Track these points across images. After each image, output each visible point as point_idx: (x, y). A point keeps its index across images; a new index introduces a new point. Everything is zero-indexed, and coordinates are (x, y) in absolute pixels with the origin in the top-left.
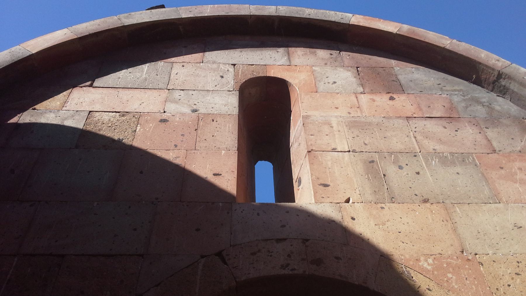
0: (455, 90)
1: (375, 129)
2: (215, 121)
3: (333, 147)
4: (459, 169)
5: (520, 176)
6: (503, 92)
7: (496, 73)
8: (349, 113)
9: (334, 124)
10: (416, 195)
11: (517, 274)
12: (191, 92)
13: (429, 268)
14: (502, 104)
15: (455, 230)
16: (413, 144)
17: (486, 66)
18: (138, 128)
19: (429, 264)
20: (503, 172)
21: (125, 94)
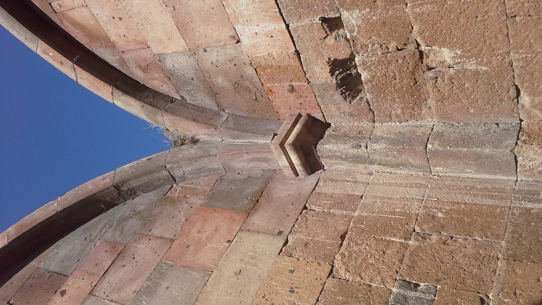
0: (101, 230)
4: (165, 284)
6: (133, 193)
7: (113, 188)
14: (141, 202)
17: (100, 191)
20: (192, 248)
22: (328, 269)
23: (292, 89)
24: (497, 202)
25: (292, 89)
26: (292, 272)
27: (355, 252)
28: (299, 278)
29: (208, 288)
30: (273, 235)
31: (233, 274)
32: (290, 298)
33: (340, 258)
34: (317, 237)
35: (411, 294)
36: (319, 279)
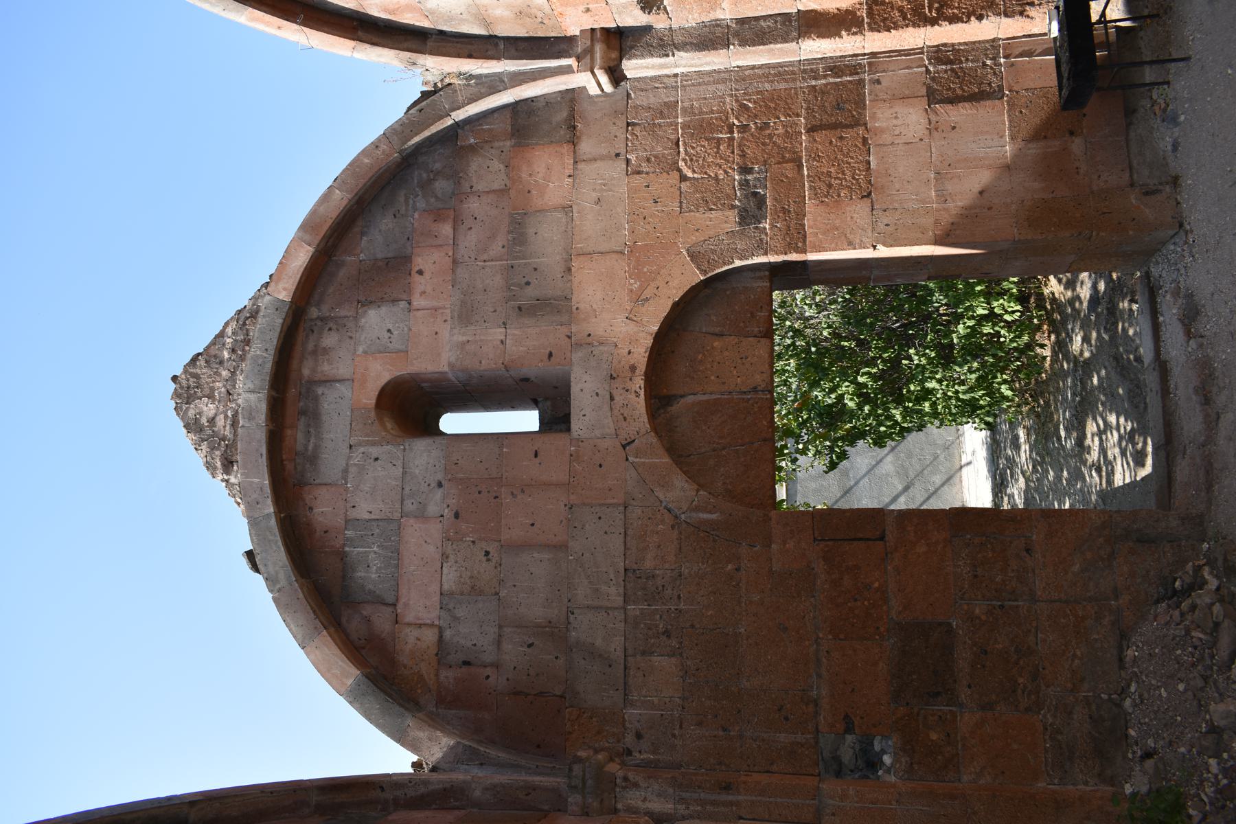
9: (465, 338)
12: (407, 491)
20: (534, 192)
22: (676, 175)
23: (588, 10)
24: (791, 85)
25: (588, 10)
35: (749, 177)
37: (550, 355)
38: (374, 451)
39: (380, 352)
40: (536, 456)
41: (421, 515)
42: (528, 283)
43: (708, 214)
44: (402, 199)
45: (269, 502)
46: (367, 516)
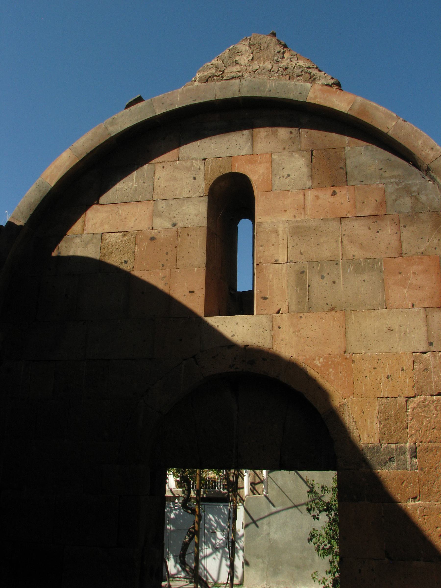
0: (393, 177)
1: (312, 235)
2: (189, 235)
3: (276, 258)
4: (366, 276)
5: (412, 280)
8: (295, 216)
9: (280, 232)
10: (327, 304)
11: (374, 368)
12: (171, 202)
13: (319, 365)
15: (345, 334)
16: (339, 251)
18: (136, 248)
19: (320, 362)
20: (399, 277)
21: (124, 210)
26: (402, 370)
27: (429, 408)
28: (399, 377)
29: (374, 313)
30: (428, 339)
31: (389, 326)
32: (383, 378)
33: (421, 399)
34: (435, 375)
35: (408, 455)
36: (402, 392)
37: (265, 298)
38: (200, 177)
39: (272, 171)
40: (191, 292)
41: (155, 214)
42: (323, 277)
43: (376, 420)
44: (395, 173)
45: (164, 111)
46: (157, 176)
